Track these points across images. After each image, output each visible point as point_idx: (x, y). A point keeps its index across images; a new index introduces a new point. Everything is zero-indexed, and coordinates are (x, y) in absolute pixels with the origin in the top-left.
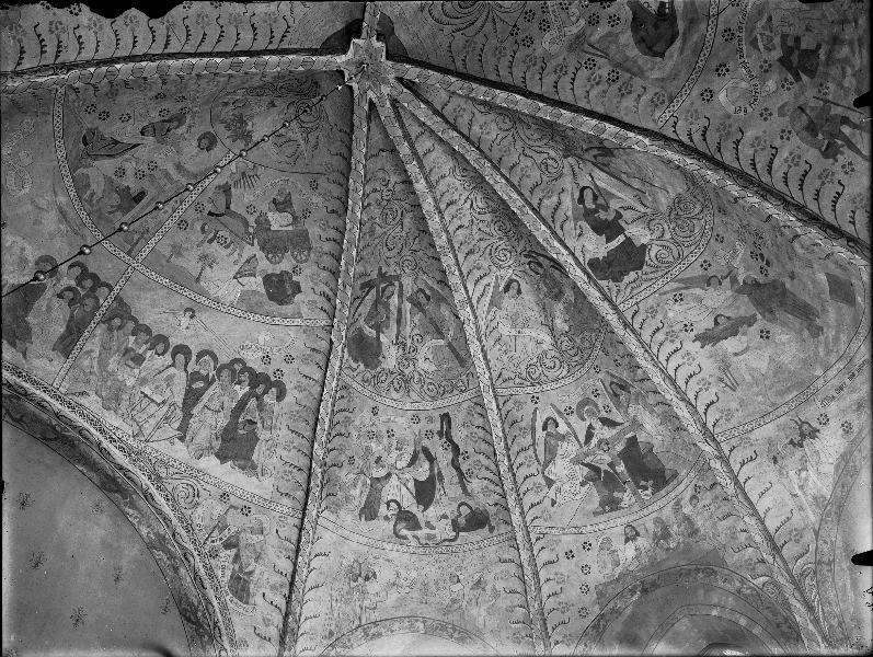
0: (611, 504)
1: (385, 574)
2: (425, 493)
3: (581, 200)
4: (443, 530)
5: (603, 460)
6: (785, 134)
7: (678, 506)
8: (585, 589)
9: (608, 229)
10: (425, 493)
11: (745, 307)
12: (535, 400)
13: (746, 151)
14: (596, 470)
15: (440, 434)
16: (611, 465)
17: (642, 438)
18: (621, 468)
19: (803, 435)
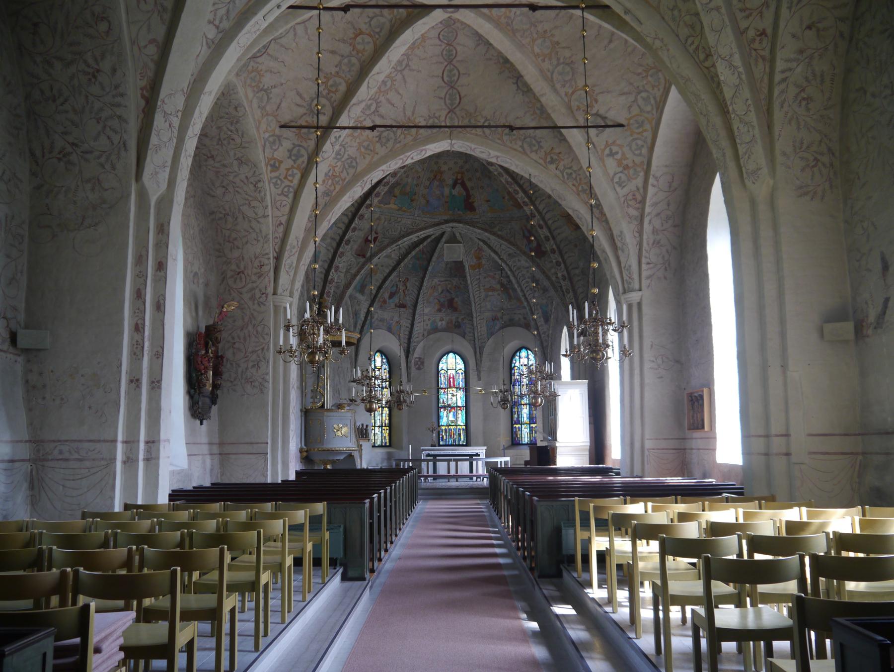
0: (439, 310)
1: (376, 316)
2: (392, 295)
3: (476, 251)
4: (393, 305)
5: (442, 300)
6: (529, 278)
7: (458, 318)
8: (425, 330)
9: (479, 258)
10: (392, 295)
11: (498, 287)
12: (433, 281)
13: (520, 274)
14: (439, 301)
15: (403, 282)
16: (444, 301)
17: (456, 299)
18: (446, 303)
19: (495, 318)
